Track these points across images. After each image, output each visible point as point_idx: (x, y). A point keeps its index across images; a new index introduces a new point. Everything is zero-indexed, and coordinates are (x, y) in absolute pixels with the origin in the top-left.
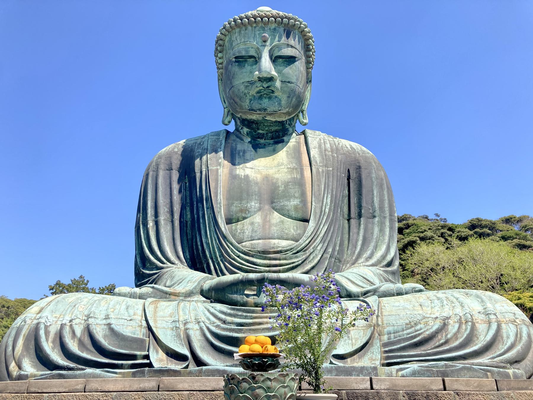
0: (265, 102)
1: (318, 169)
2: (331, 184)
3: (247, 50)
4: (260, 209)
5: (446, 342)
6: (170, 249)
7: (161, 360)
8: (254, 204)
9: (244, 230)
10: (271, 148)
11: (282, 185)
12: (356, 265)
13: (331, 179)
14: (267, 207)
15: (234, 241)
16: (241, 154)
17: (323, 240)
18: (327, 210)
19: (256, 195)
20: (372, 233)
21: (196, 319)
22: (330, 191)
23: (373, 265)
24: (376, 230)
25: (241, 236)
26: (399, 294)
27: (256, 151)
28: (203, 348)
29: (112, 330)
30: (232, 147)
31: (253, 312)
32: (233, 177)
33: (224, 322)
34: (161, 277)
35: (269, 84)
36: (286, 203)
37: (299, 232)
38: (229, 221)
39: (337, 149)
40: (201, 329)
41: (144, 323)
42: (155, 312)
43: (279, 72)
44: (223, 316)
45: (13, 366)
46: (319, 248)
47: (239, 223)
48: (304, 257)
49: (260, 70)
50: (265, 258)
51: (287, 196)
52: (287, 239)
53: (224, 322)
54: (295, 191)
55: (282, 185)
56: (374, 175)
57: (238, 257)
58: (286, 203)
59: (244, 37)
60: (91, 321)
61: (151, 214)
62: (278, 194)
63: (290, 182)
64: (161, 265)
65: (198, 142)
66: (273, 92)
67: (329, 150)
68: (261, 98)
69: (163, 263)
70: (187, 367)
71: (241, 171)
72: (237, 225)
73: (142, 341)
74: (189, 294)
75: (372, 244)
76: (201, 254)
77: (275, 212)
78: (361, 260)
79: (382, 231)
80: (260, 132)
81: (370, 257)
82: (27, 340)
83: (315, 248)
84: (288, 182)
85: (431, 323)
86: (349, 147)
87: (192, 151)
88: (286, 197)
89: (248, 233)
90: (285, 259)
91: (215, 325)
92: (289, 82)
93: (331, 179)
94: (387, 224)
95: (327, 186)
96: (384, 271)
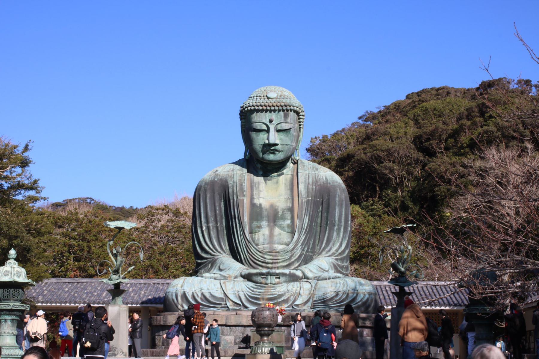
1: (302, 200)
3: (261, 127)
4: (268, 225)
5: (336, 301)
7: (231, 306)
8: (264, 223)
10: (274, 180)
12: (321, 256)
13: (309, 206)
14: (272, 224)
15: (254, 245)
17: (302, 245)
20: (333, 236)
22: (308, 214)
23: (329, 256)
25: (258, 242)
26: (329, 279)
29: (211, 295)
30: (251, 179)
31: (265, 287)
32: (253, 205)
33: (253, 291)
35: (274, 148)
37: (289, 240)
38: (251, 232)
39: (317, 181)
42: (226, 287)
43: (281, 139)
44: (252, 289)
45: (179, 307)
50: (271, 255)
51: (283, 218)
52: (282, 244)
54: (288, 215)
56: (337, 199)
58: (282, 223)
59: (259, 117)
64: (213, 253)
67: (311, 183)
73: (222, 299)
75: (332, 243)
78: (324, 253)
79: (338, 234)
80: (269, 168)
81: (329, 251)
82: (182, 297)
83: (297, 250)
86: (324, 178)
87: (226, 182)
89: (261, 240)
90: (281, 256)
93: (309, 206)
94: (342, 230)
95: (307, 210)
96: (337, 259)
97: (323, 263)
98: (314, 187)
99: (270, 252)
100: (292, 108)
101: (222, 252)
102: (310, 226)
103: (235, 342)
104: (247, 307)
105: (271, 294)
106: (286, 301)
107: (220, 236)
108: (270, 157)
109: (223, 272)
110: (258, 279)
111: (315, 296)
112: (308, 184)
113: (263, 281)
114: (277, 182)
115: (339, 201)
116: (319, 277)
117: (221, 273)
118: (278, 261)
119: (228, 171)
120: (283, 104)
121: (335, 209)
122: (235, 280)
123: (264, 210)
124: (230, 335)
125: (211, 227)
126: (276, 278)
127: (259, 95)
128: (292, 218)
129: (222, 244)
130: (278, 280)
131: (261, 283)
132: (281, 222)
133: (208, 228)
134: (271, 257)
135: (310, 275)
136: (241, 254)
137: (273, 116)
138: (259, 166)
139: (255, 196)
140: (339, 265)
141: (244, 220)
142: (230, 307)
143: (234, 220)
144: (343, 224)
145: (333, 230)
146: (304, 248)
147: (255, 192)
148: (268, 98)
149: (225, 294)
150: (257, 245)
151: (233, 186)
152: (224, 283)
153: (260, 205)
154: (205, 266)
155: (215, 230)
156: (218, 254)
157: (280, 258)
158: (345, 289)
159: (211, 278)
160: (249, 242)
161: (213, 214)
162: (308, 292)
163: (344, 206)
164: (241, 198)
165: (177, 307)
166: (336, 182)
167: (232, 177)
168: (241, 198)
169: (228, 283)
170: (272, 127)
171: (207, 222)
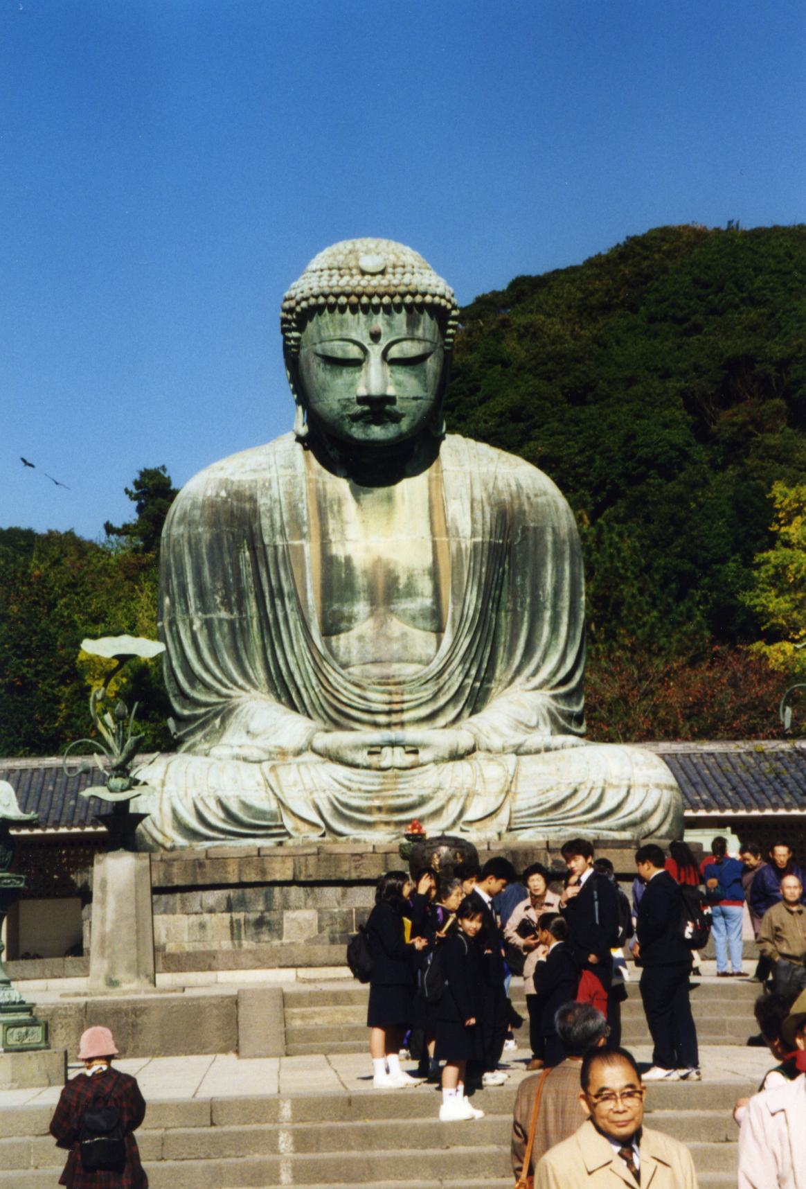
0: (377, 432)
1: (459, 543)
2: (478, 567)
3: (344, 351)
6: (233, 663)
7: (296, 829)
8: (361, 608)
10: (380, 492)
13: (479, 559)
14: (381, 610)
15: (336, 666)
16: (335, 507)
17: (463, 661)
18: (471, 613)
23: (536, 689)
24: (546, 630)
26: (548, 750)
27: (358, 501)
28: (333, 816)
30: (318, 490)
32: (328, 561)
33: (350, 789)
34: (231, 711)
40: (329, 799)
41: (272, 795)
43: (398, 384)
44: (347, 783)
45: (160, 838)
46: (457, 673)
47: (342, 636)
48: (436, 688)
49: (367, 387)
50: (383, 692)
51: (411, 592)
52: (412, 661)
53: (350, 789)
54: (425, 585)
57: (345, 689)
60: (220, 794)
62: (398, 590)
64: (224, 691)
65: (260, 484)
68: (368, 423)
69: (226, 686)
70: (323, 835)
72: (338, 639)
74: (299, 753)
76: (286, 678)
77: (395, 619)
81: (534, 674)
83: (453, 673)
85: (563, 788)
87: (252, 499)
89: (355, 656)
90: (411, 692)
93: (479, 559)
97: (519, 704)
98: (487, 509)
99: (379, 684)
100: (428, 299)
101: (248, 687)
102: (483, 613)
103: (321, 929)
104: (341, 835)
105: (398, 796)
106: (437, 813)
107: (240, 644)
108: (369, 432)
109: (259, 738)
110: (362, 757)
111: (519, 797)
112: (472, 501)
113: (374, 760)
114: (390, 499)
115: (555, 543)
116: (520, 745)
117: (259, 742)
118: (405, 706)
119: (255, 471)
120: (402, 289)
121: (544, 565)
122: (299, 759)
123: (358, 572)
124: (306, 907)
125: (216, 622)
126: (408, 753)
127: (336, 264)
129: (247, 665)
130: (411, 759)
131: (368, 767)
133: (208, 624)
134: (386, 698)
135: (496, 742)
136: (303, 690)
137: (379, 321)
138: (334, 453)
139: (332, 537)
140: (562, 713)
141: (306, 601)
142: (293, 833)
143: (278, 602)
144: (565, 603)
145: (542, 620)
147: (332, 524)
148: (363, 273)
149: (279, 800)
150: (345, 666)
151: (271, 510)
152: (273, 768)
153: (348, 560)
154: (202, 726)
155: (226, 628)
156: (235, 692)
157: (406, 697)
158: (593, 777)
159: (237, 758)
160: (323, 658)
161: (219, 585)
162: (495, 788)
163: (567, 554)
164: (297, 543)
165: (155, 840)
166: (545, 494)
167: (267, 487)
168: (297, 543)
169: (281, 771)
170: (375, 351)
171: (205, 608)
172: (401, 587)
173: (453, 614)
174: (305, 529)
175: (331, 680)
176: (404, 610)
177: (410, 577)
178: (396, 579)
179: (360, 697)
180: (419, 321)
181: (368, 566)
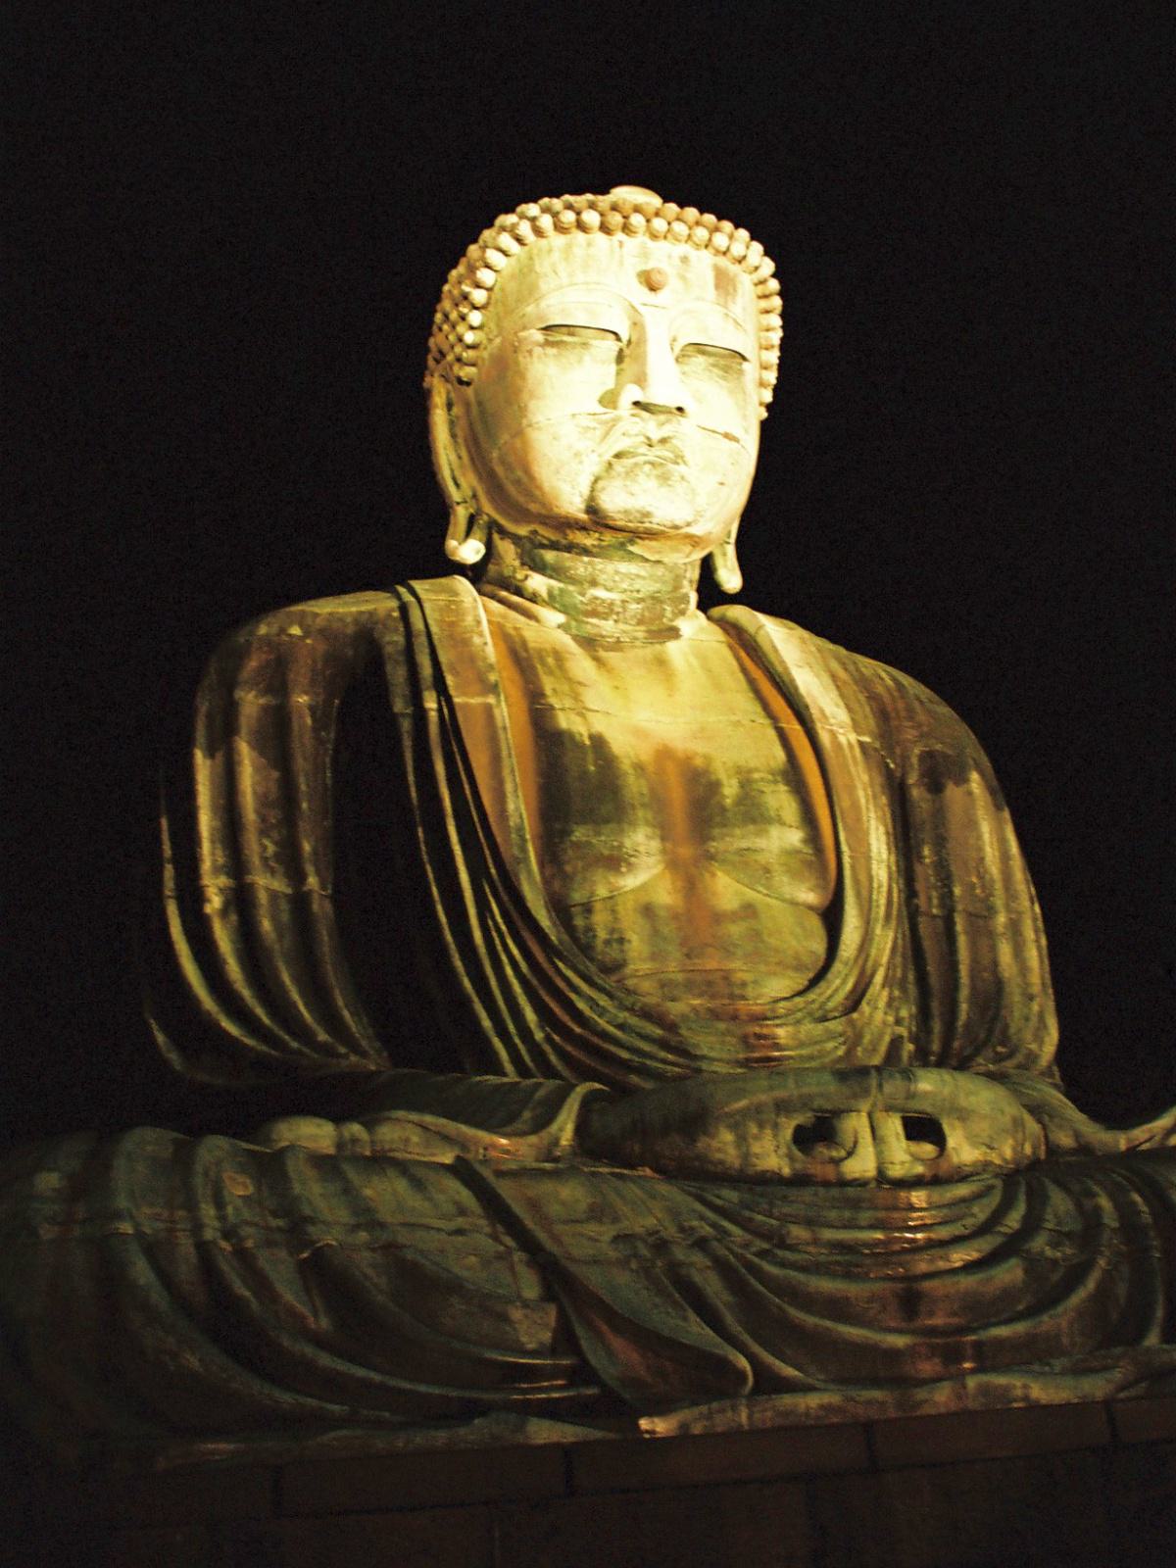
1: (833, 734)
9: (620, 931)
11: (729, 777)
14: (686, 851)
15: (593, 969)
16: (550, 660)
19: (643, 805)
21: (682, 1229)
25: (614, 953)
27: (597, 659)
36: (760, 843)
51: (752, 812)
54: (781, 800)
55: (729, 777)
61: (214, 861)
62: (723, 810)
63: (757, 770)
66: (678, 459)
71: (578, 719)
84: (750, 771)
88: (754, 821)
91: (754, 1249)
92: (727, 436)
101: (343, 1050)
123: (626, 766)
128: (809, 818)
132: (738, 839)
139: (553, 701)
146: (898, 1010)
153: (599, 742)
164: (475, 701)
168: (475, 701)
172: (728, 801)
173: (853, 867)
174: (493, 677)
175: (581, 1005)
176: (742, 852)
177: (746, 784)
178: (714, 787)
179: (663, 1044)
180: (735, 290)
181: (645, 754)
